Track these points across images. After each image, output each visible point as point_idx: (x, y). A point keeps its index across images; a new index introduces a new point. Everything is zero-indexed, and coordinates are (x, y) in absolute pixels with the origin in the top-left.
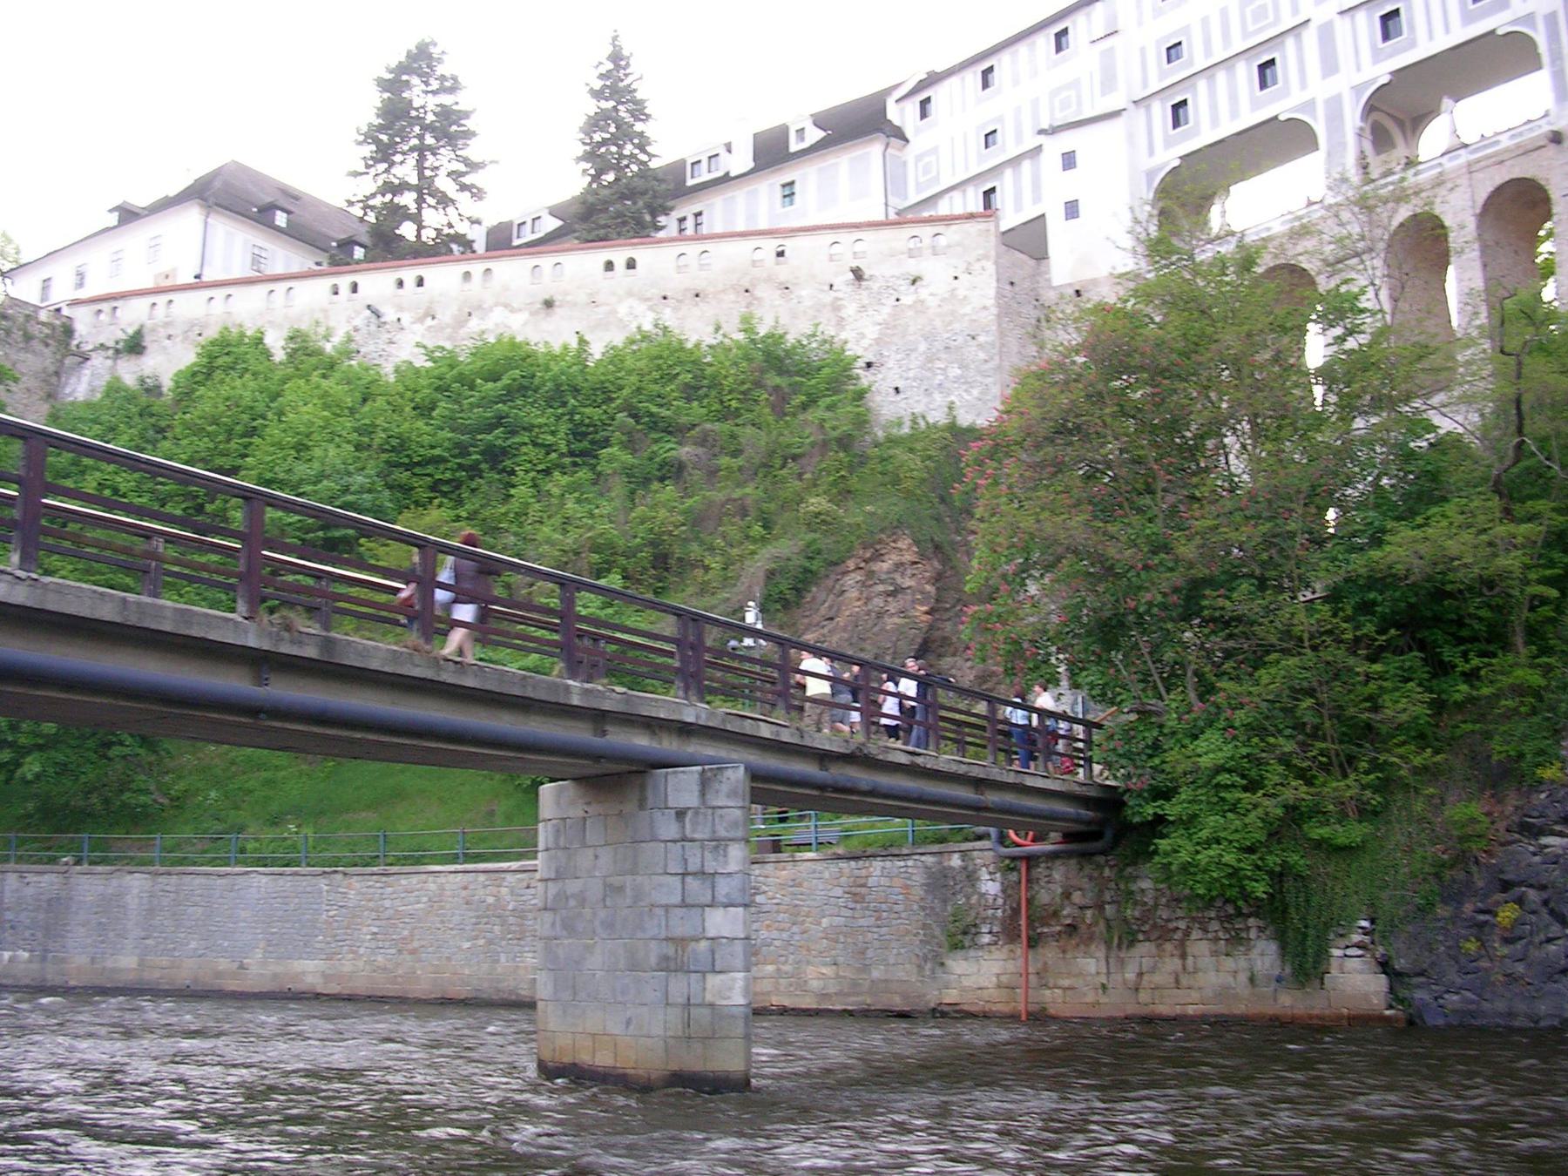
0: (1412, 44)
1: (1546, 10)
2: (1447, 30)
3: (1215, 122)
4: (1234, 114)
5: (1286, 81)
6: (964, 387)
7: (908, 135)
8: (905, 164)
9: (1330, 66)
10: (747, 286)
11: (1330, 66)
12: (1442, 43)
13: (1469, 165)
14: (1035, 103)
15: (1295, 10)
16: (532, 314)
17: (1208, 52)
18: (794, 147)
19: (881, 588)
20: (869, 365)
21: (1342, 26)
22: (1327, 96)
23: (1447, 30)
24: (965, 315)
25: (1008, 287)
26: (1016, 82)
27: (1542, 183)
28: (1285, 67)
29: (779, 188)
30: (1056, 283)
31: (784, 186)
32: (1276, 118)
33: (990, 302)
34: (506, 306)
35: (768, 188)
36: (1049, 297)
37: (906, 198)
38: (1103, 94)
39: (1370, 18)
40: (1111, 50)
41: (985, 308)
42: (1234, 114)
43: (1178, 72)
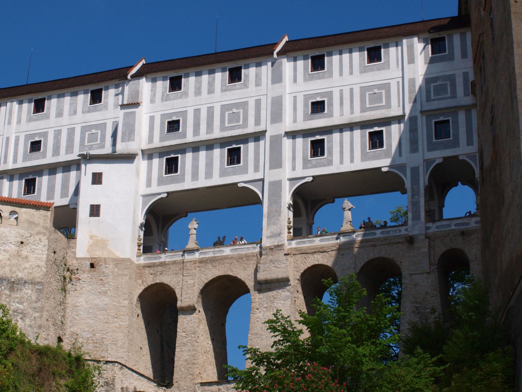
0: (330, 163)
1: (413, 165)
2: (352, 161)
3: (195, 176)
4: (209, 175)
5: (246, 162)
6: (21, 316)
12: (347, 167)
14: (71, 132)
15: (258, 122)
17: (196, 130)
21: (287, 142)
22: (272, 179)
23: (352, 161)
24: (25, 268)
25: (52, 254)
26: (60, 114)
27: (398, 263)
28: (247, 155)
30: (79, 255)
32: (235, 184)
33: (43, 264)
36: (73, 263)
38: (122, 141)
41: (38, 266)
42: (209, 175)
43: (174, 141)
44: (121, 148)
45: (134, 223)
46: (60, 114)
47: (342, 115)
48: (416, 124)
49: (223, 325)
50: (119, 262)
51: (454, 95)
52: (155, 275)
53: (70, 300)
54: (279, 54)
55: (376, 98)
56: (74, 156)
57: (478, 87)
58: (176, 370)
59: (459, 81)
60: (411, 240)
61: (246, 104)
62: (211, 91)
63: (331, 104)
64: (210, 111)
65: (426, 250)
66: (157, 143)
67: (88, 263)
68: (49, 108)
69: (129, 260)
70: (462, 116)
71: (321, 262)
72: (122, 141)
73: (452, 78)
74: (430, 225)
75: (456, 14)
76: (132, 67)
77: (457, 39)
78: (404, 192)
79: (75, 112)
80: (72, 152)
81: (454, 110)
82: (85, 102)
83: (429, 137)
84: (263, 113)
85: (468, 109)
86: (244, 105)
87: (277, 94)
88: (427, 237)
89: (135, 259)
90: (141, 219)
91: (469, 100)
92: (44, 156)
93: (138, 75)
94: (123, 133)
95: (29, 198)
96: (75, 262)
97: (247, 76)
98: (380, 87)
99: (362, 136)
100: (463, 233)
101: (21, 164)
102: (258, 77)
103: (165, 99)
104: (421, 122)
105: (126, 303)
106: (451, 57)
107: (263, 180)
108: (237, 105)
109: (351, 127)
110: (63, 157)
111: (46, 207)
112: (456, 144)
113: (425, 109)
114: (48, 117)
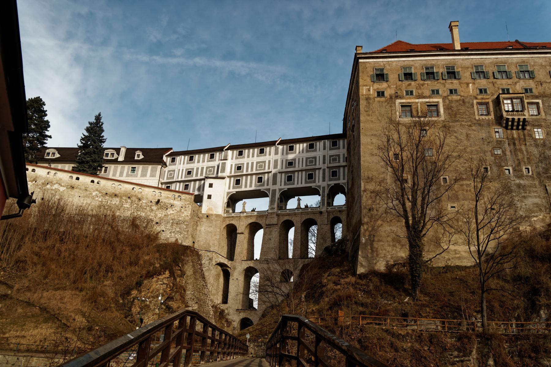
0: (294, 184)
2: (301, 183)
3: (246, 186)
4: (251, 186)
7: (168, 164)
8: (165, 171)
9: (275, 183)
10: (129, 196)
11: (275, 183)
12: (300, 185)
13: (301, 212)
14: (202, 168)
15: (269, 168)
16: (67, 188)
17: (247, 170)
18: (136, 158)
19: (160, 283)
20: (157, 223)
22: (273, 189)
23: (301, 183)
26: (199, 162)
29: (131, 168)
30: (203, 212)
31: (132, 168)
34: (59, 184)
35: (127, 168)
36: (200, 215)
37: (164, 180)
38: (221, 172)
39: (285, 176)
40: (225, 163)
42: (251, 186)
44: (220, 175)
45: (223, 202)
46: (199, 162)
47: (299, 167)
48: (325, 171)
49: (253, 240)
50: (217, 216)
51: (339, 161)
52: (230, 220)
53: (198, 228)
54: (278, 144)
55: (311, 162)
56: (203, 177)
57: (348, 159)
58: (235, 255)
59: (341, 157)
60: (321, 213)
61: (265, 161)
62: (253, 156)
63: (295, 163)
64: (252, 163)
65: (326, 216)
66: (233, 174)
67: (206, 216)
68: (195, 160)
69: (221, 215)
70: (342, 169)
71: (289, 219)
72: (221, 172)
73: (339, 156)
74: (328, 207)
75: (342, 133)
76: (225, 147)
77: (341, 142)
78: (320, 195)
79: (204, 162)
80: (202, 176)
81: (339, 167)
82: (208, 158)
83: (329, 176)
84: (271, 165)
85: (344, 167)
86: (264, 162)
87: (276, 159)
88: (327, 211)
89: (223, 215)
90: (226, 201)
91: (344, 164)
92: (192, 176)
93: (228, 149)
94: (221, 170)
95: (186, 191)
96: (201, 215)
97: (266, 152)
98: (313, 158)
99: (306, 175)
100: (340, 211)
101: (183, 179)
102: (270, 152)
103: (237, 158)
104: (327, 171)
105: (219, 230)
106: (339, 148)
107: (269, 189)
108: (262, 162)
109: (302, 171)
110: (199, 177)
111: (192, 194)
112: (339, 179)
113: (329, 166)
114: (194, 162)
